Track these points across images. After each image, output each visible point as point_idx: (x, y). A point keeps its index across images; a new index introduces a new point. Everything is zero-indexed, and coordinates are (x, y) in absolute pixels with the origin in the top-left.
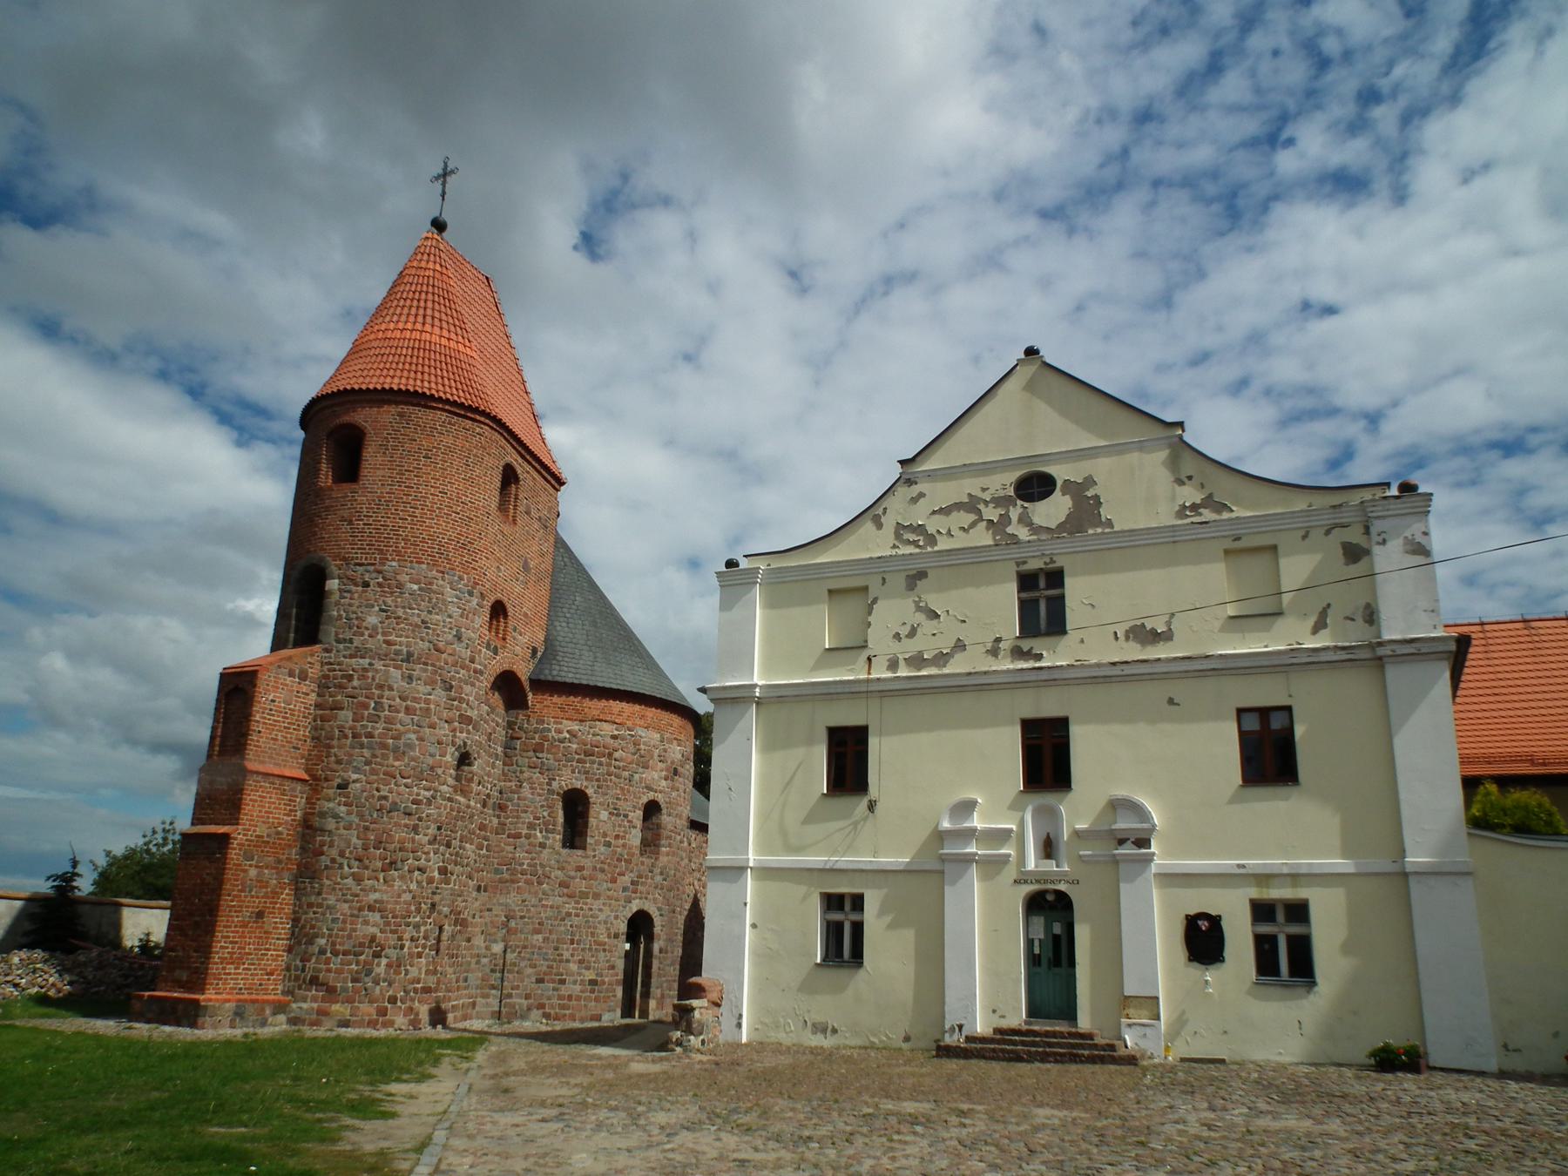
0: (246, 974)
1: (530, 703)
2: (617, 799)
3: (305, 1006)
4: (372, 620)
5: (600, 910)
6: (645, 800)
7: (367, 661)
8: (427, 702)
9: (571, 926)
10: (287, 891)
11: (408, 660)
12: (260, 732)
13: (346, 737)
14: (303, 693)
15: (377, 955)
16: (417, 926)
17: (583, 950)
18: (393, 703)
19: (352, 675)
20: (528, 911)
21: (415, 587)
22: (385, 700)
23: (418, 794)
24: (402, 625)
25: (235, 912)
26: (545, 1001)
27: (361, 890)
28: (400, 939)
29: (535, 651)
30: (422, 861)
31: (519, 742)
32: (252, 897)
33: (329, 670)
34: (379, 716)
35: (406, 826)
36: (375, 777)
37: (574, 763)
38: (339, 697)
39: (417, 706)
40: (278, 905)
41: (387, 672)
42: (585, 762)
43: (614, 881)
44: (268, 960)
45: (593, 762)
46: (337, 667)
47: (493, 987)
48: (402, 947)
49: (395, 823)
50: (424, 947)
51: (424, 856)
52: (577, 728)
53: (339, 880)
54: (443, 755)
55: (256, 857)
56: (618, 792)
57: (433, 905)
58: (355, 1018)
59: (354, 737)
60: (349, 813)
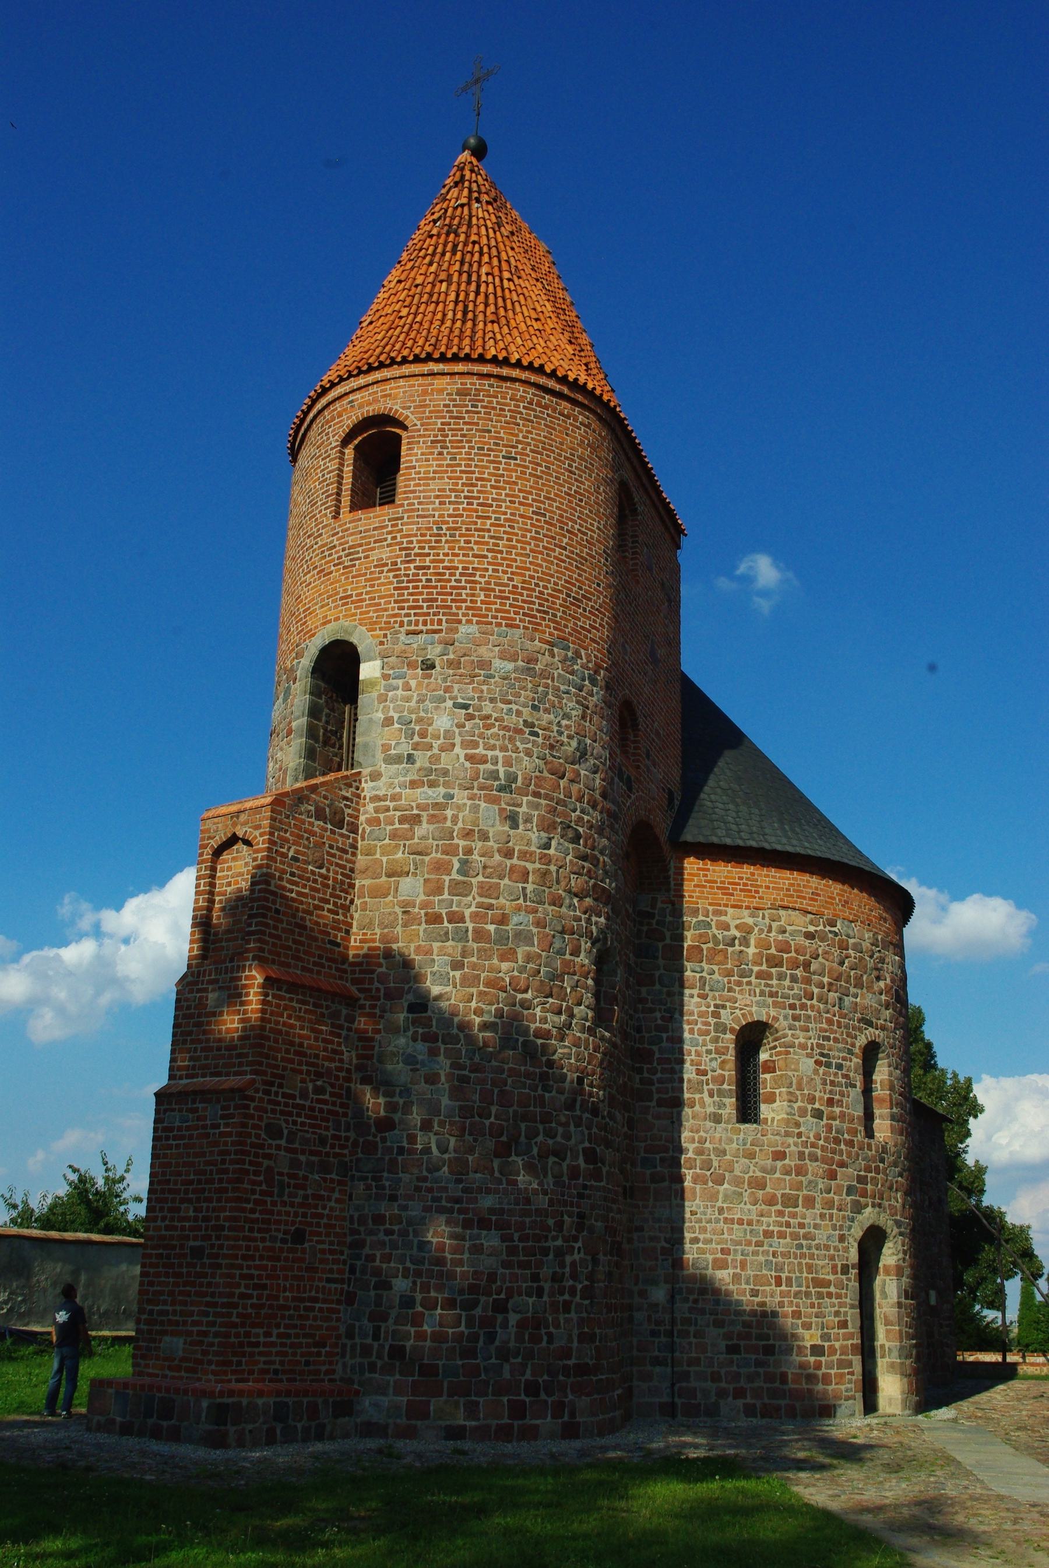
0: (283, 1345)
1: (672, 883)
2: (828, 1039)
3: (385, 1401)
4: (443, 722)
5: (816, 1226)
6: (862, 1041)
7: (442, 790)
8: (546, 860)
9: (774, 1254)
10: (336, 1195)
12: (277, 911)
14: (338, 849)
15: (500, 1307)
16: (560, 1253)
17: (797, 1295)
18: (489, 864)
19: (418, 816)
20: (704, 1230)
21: (510, 666)
23: (544, 1020)
24: (495, 730)
25: (260, 1231)
26: (742, 1383)
27: (465, 1190)
28: (535, 1278)
29: (671, 793)
30: (559, 1139)
31: (660, 945)
32: (284, 1204)
35: (528, 1075)
36: (474, 990)
37: (753, 979)
38: (400, 855)
39: (530, 866)
40: (325, 1221)
41: (475, 809)
42: (769, 976)
43: (832, 1176)
44: (315, 1319)
45: (781, 977)
46: (392, 805)
47: (657, 1362)
48: (540, 1293)
49: (510, 1069)
50: (573, 1291)
51: (560, 1130)
52: (750, 921)
53: (425, 1173)
54: (576, 952)
55: (286, 1132)
56: (824, 1026)
57: (581, 1216)
58: (474, 1423)
60: (433, 1053)
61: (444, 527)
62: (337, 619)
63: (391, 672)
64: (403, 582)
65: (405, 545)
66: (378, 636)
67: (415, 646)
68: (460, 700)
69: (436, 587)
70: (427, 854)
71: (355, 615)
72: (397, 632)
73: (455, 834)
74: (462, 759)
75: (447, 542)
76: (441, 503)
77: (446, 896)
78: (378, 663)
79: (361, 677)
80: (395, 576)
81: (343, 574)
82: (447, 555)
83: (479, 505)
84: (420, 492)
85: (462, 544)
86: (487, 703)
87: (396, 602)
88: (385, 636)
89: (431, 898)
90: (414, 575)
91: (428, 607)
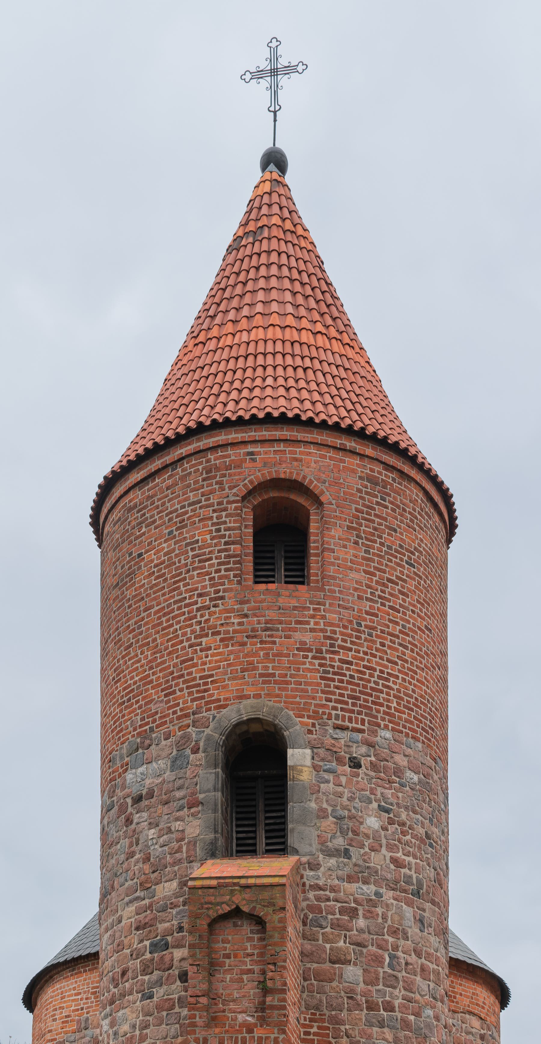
7: (373, 888)
11: (417, 893)
13: (358, 1007)
18: (410, 960)
19: (356, 909)
22: (400, 954)
33: (318, 899)
34: (396, 978)
38: (341, 944)
46: (332, 895)
59: (369, 1008)
61: (363, 623)
62: (258, 696)
63: (321, 763)
64: (328, 672)
65: (329, 634)
66: (307, 724)
67: (342, 742)
68: (383, 804)
69: (358, 685)
70: (365, 946)
71: (278, 696)
72: (325, 724)
73: (386, 930)
74: (388, 861)
75: (366, 640)
76: (360, 597)
77: (381, 987)
78: (308, 751)
79: (290, 763)
80: (321, 665)
81: (262, 649)
82: (365, 653)
83: (391, 607)
84: (341, 580)
85: (378, 646)
86: (402, 810)
87: (323, 692)
88: (314, 725)
89: (370, 987)
90: (339, 667)
91: (354, 705)
